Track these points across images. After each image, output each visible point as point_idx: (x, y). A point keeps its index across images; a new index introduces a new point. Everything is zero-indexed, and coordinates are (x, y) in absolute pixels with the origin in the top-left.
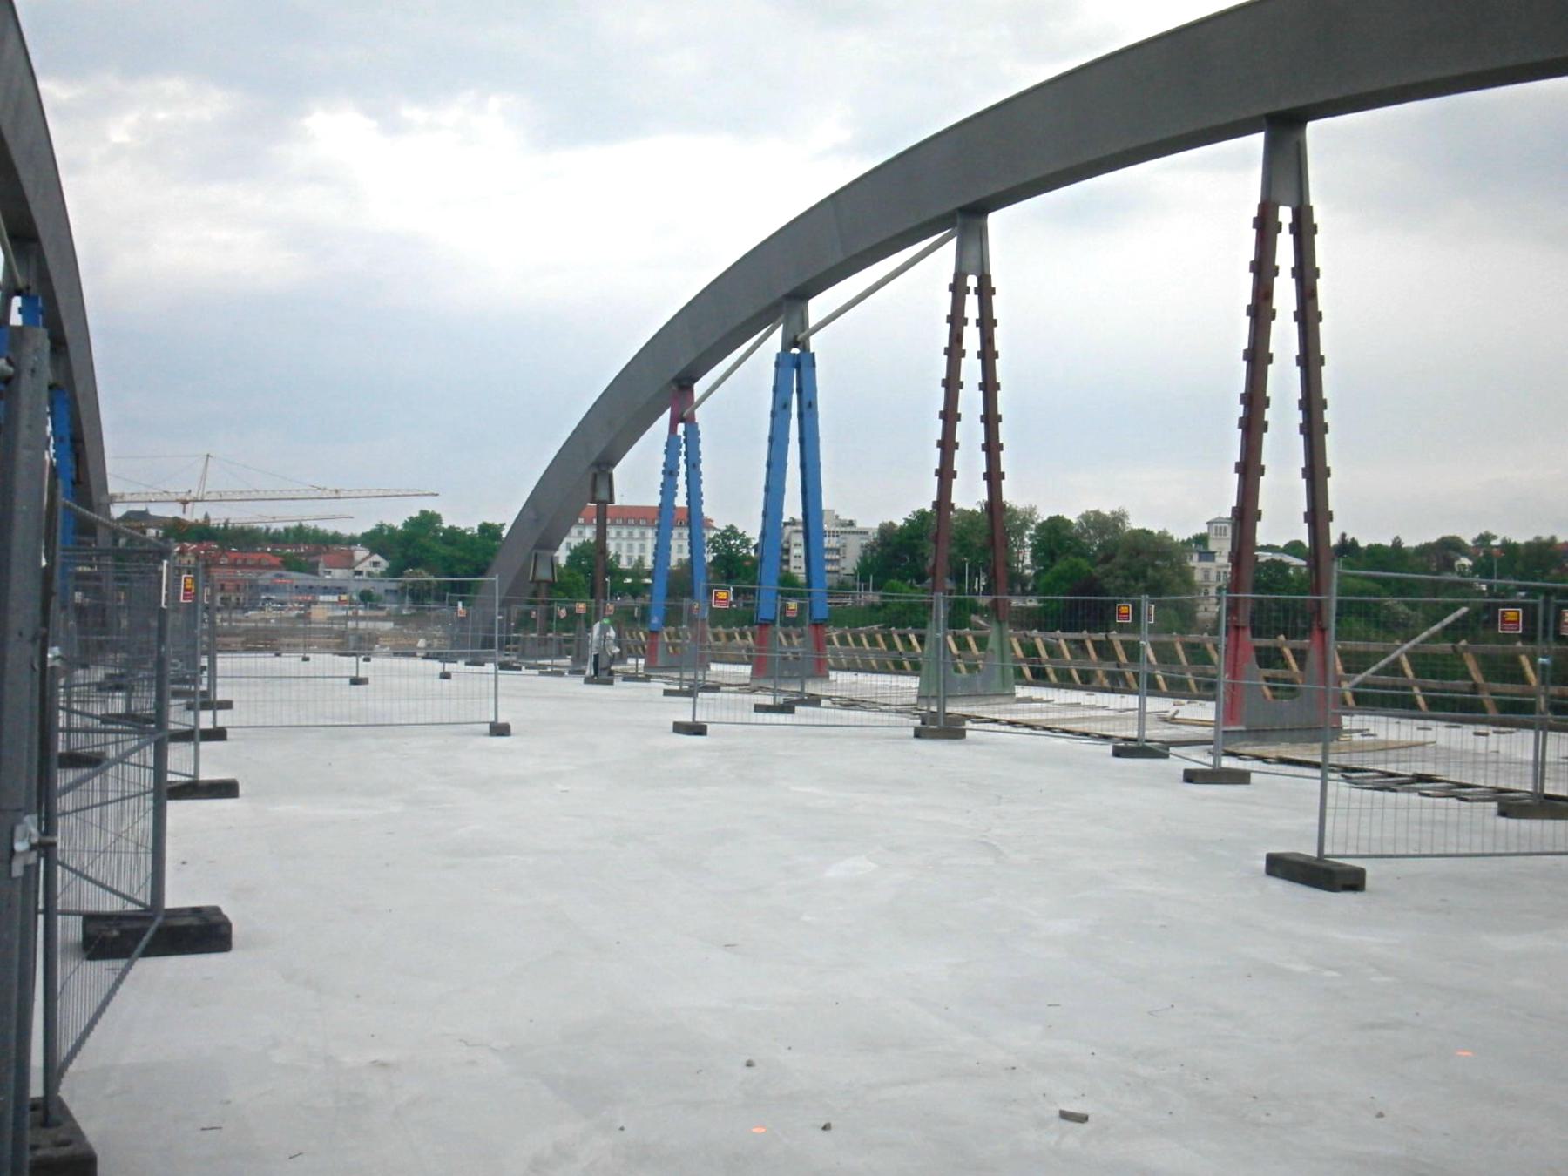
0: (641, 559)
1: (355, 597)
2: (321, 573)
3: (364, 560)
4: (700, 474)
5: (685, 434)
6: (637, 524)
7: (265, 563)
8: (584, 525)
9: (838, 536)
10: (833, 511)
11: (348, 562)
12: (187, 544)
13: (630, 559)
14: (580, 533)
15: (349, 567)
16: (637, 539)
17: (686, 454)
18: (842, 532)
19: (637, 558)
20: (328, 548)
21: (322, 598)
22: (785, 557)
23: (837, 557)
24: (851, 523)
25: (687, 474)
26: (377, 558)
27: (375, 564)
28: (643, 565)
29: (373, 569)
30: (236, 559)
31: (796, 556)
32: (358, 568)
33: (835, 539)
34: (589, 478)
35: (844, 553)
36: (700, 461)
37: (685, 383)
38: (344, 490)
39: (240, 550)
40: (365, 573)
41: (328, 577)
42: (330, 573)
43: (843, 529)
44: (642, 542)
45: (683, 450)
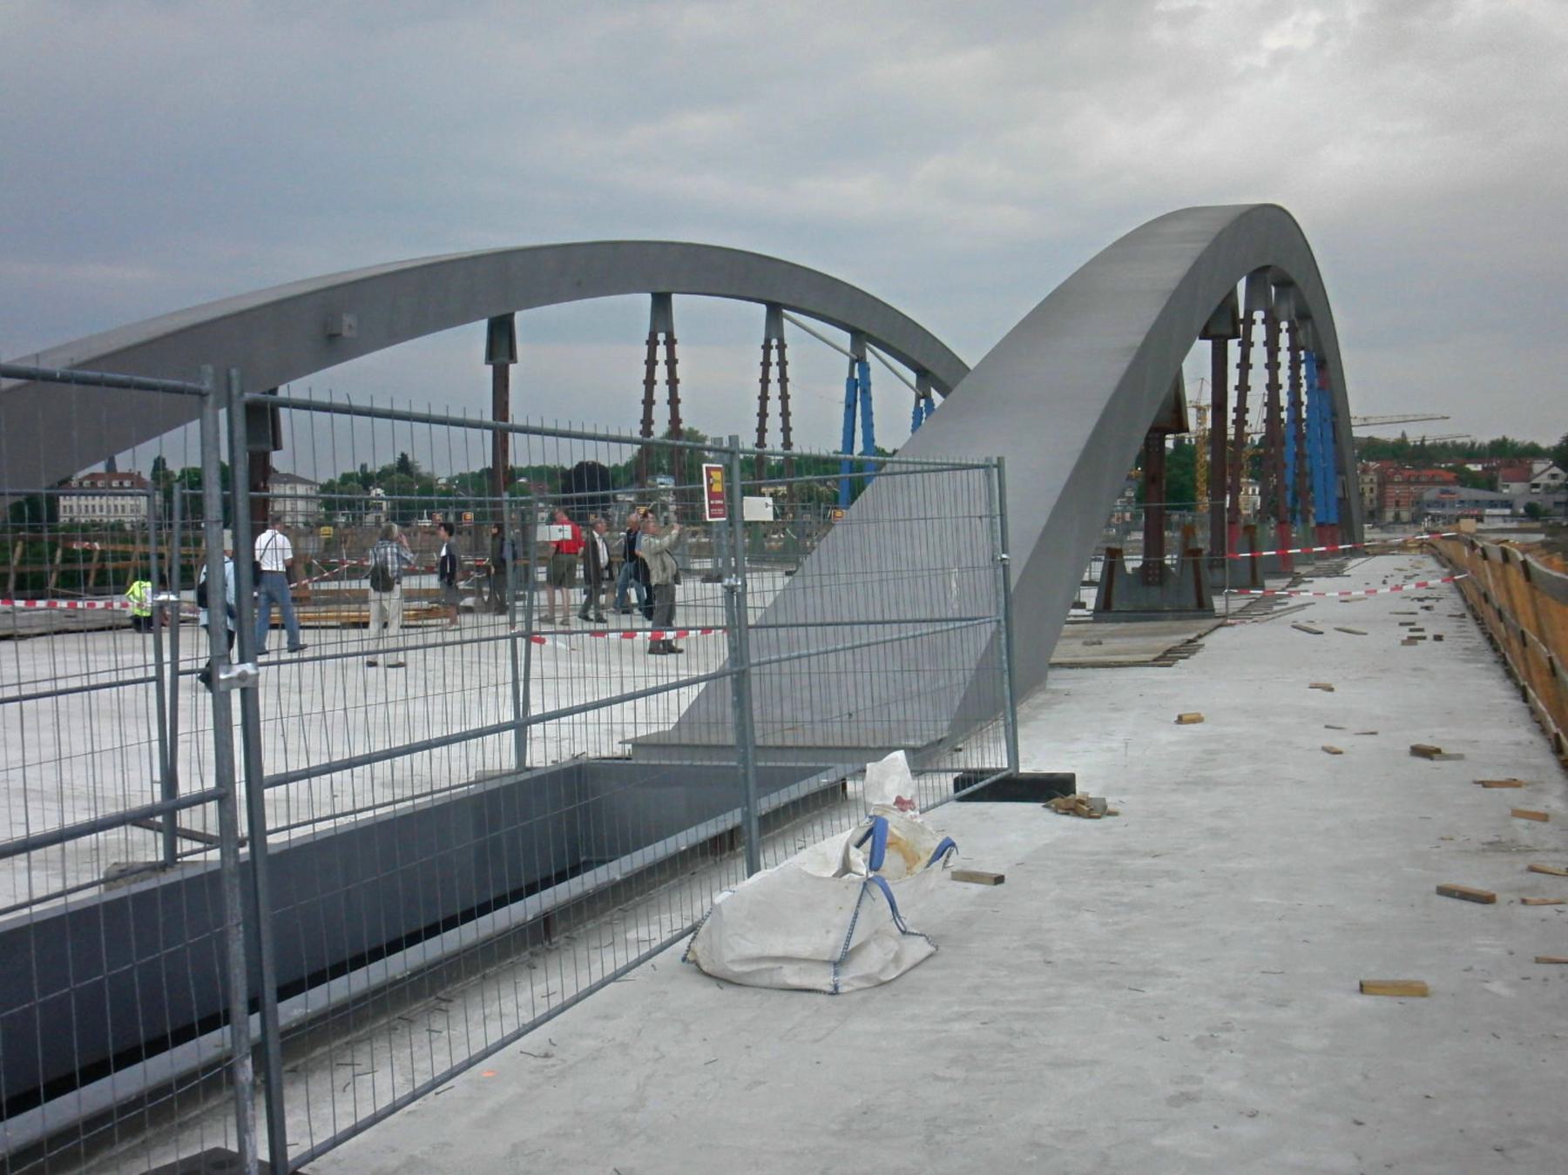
1: (1522, 511)
2: (1500, 488)
3: (1542, 472)
7: (1437, 479)
11: (1526, 476)
12: (1371, 464)
15: (1528, 481)
20: (1520, 462)
21: (1488, 511)
26: (1556, 470)
27: (1554, 476)
29: (1552, 482)
30: (1410, 476)
32: (1535, 481)
38: (1371, 418)
39: (1415, 467)
40: (1542, 487)
41: (1506, 491)
42: (1508, 487)
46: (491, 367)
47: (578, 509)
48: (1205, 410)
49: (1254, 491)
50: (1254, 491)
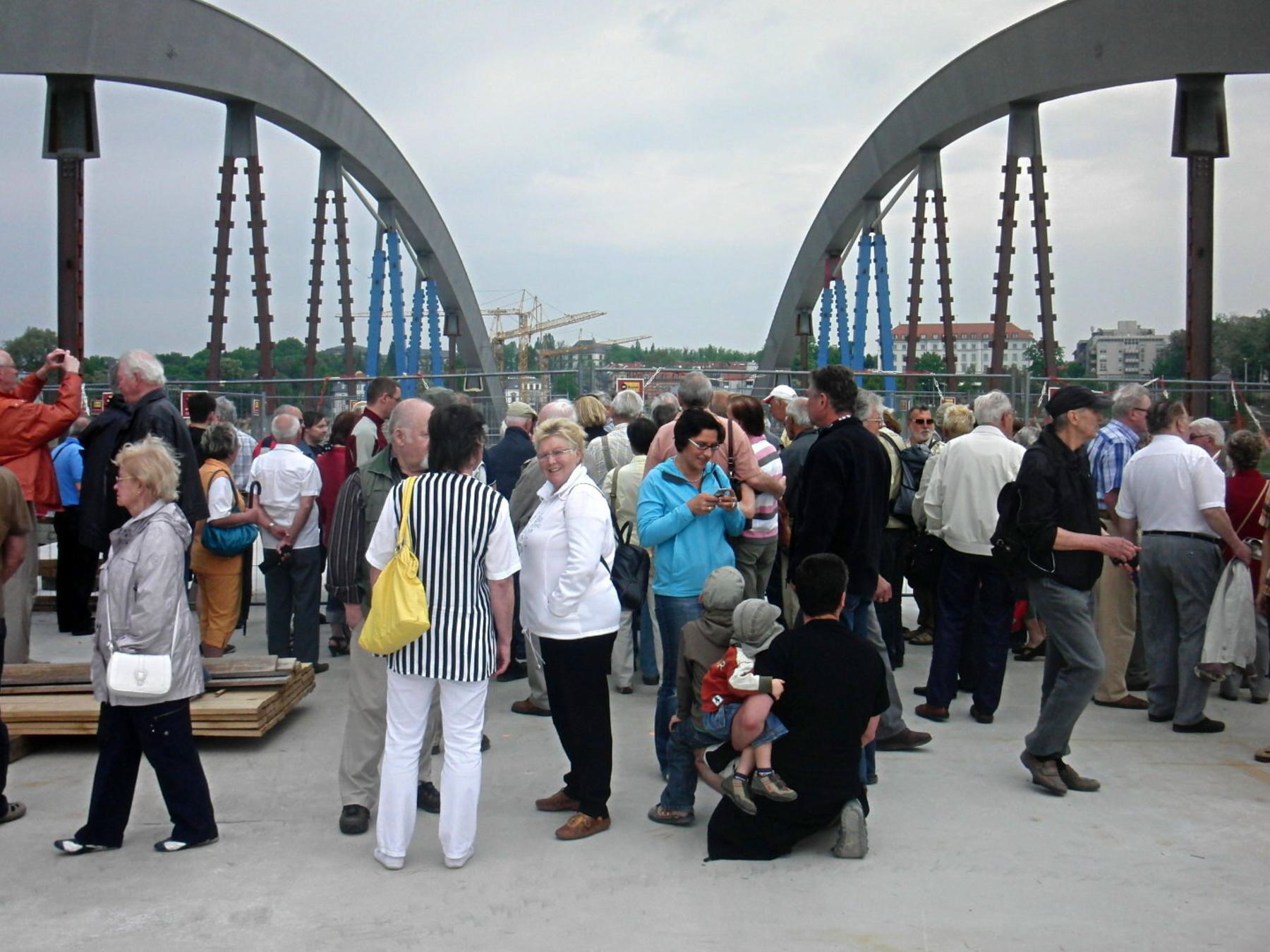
0: (973, 367)
4: (847, 315)
5: (835, 288)
6: (969, 338)
8: (926, 340)
9: (1137, 343)
10: (1135, 322)
13: (964, 366)
14: (923, 347)
16: (969, 350)
17: (836, 301)
18: (1141, 340)
19: (969, 366)
22: (1093, 362)
23: (1137, 360)
24: (1150, 332)
25: (837, 315)
28: (974, 371)
31: (1101, 361)
33: (1135, 346)
34: (795, 317)
35: (1143, 356)
36: (846, 306)
37: (834, 253)
41: (726, 387)
42: (727, 384)
43: (1143, 337)
44: (974, 353)
45: (835, 298)
46: (54, 163)
47: (1250, 387)
48: (526, 317)
49: (537, 386)
50: (537, 386)
